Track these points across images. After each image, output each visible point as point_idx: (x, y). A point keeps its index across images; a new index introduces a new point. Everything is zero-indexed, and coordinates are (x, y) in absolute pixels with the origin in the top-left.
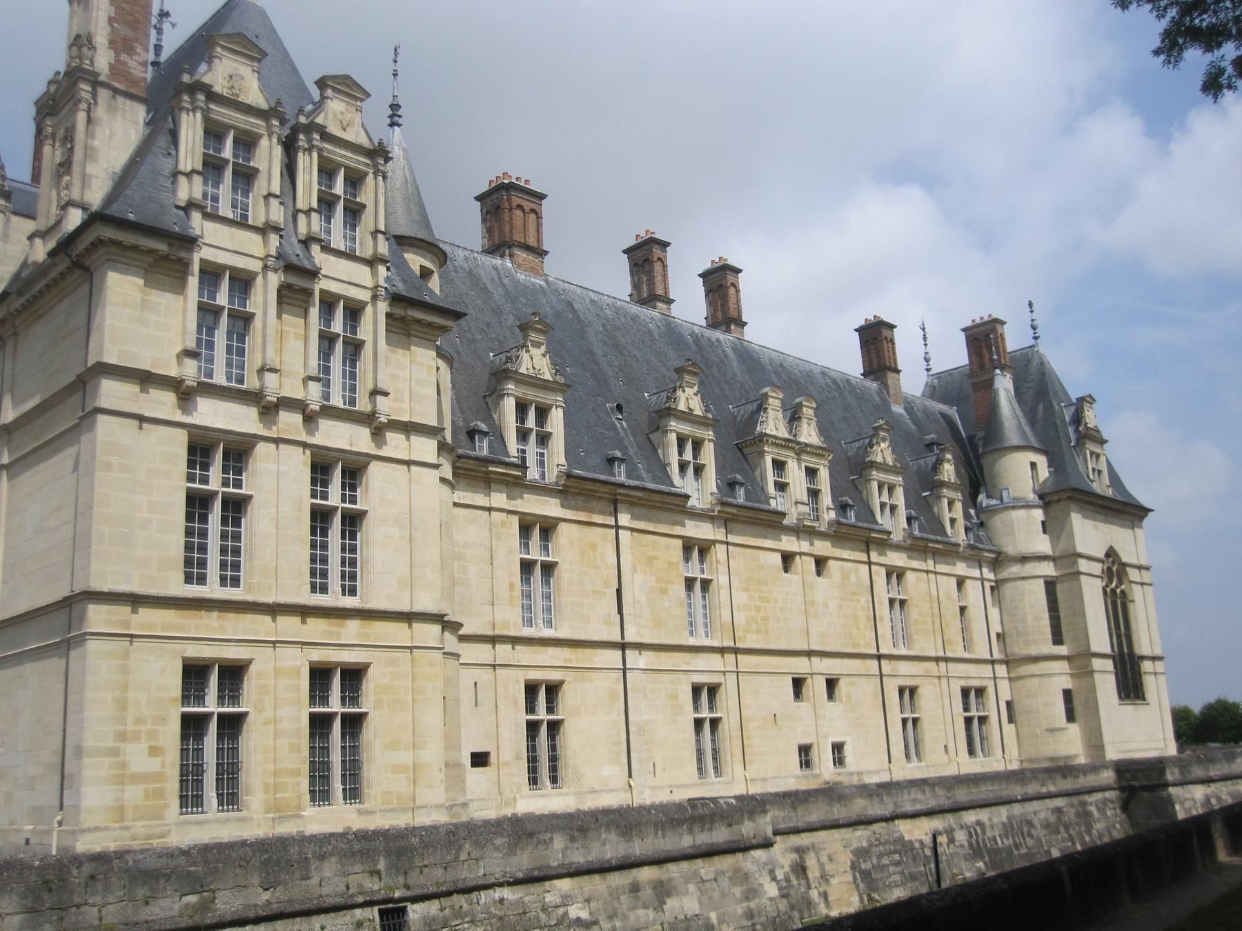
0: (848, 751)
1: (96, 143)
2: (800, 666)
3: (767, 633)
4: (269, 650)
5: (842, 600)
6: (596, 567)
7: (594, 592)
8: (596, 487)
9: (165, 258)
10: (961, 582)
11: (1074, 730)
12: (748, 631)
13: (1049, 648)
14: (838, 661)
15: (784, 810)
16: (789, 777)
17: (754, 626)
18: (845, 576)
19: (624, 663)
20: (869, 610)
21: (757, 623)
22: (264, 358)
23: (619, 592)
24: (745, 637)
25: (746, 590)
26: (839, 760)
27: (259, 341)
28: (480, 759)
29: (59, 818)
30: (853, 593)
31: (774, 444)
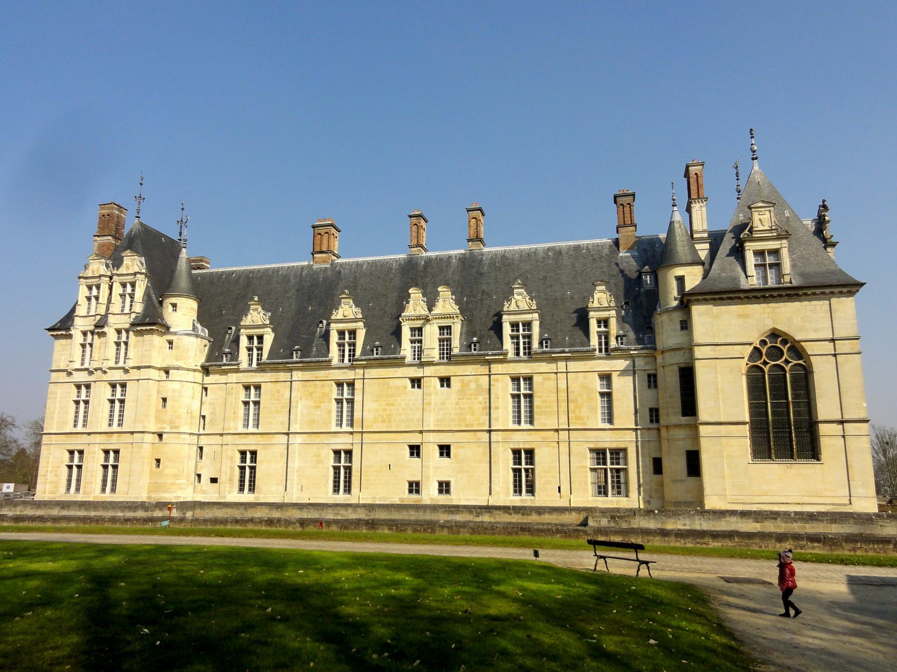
2: (415, 439)
3: (390, 422)
5: (459, 399)
6: (279, 400)
7: (276, 411)
8: (276, 366)
9: (66, 335)
10: (606, 377)
15: (239, 510)
17: (380, 419)
18: (465, 385)
19: (288, 442)
20: (486, 403)
24: (372, 425)
28: (214, 480)
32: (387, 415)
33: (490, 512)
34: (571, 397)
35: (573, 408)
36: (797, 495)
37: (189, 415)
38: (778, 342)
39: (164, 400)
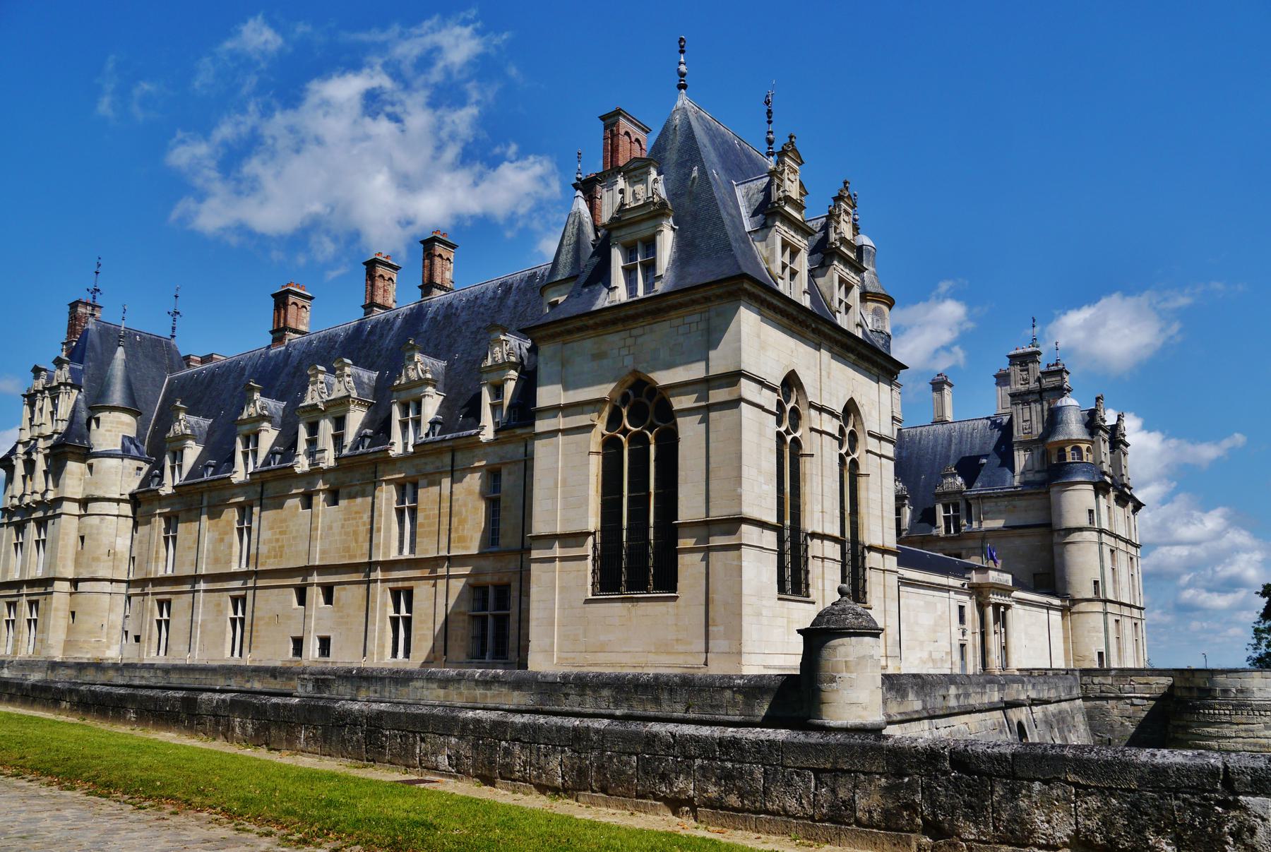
5: (345, 520)
12: (268, 557)
21: (275, 551)
25: (272, 528)
30: (356, 513)
32: (279, 547)
33: (258, 676)
34: (455, 508)
35: (456, 524)
36: (641, 650)
37: (112, 557)
38: (644, 395)
39: (82, 538)
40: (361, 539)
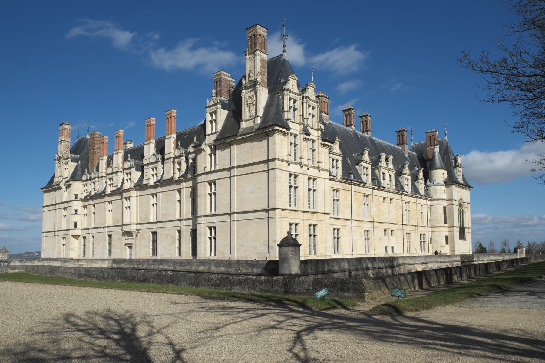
0: (395, 248)
1: (260, 100)
4: (303, 221)
7: (347, 207)
11: (447, 247)
12: (376, 217)
13: (443, 224)
14: (394, 225)
16: (382, 253)
22: (301, 155)
23: (351, 207)
25: (376, 207)
26: (393, 251)
27: (299, 151)
29: (269, 255)
31: (383, 169)
40: (399, 217)
